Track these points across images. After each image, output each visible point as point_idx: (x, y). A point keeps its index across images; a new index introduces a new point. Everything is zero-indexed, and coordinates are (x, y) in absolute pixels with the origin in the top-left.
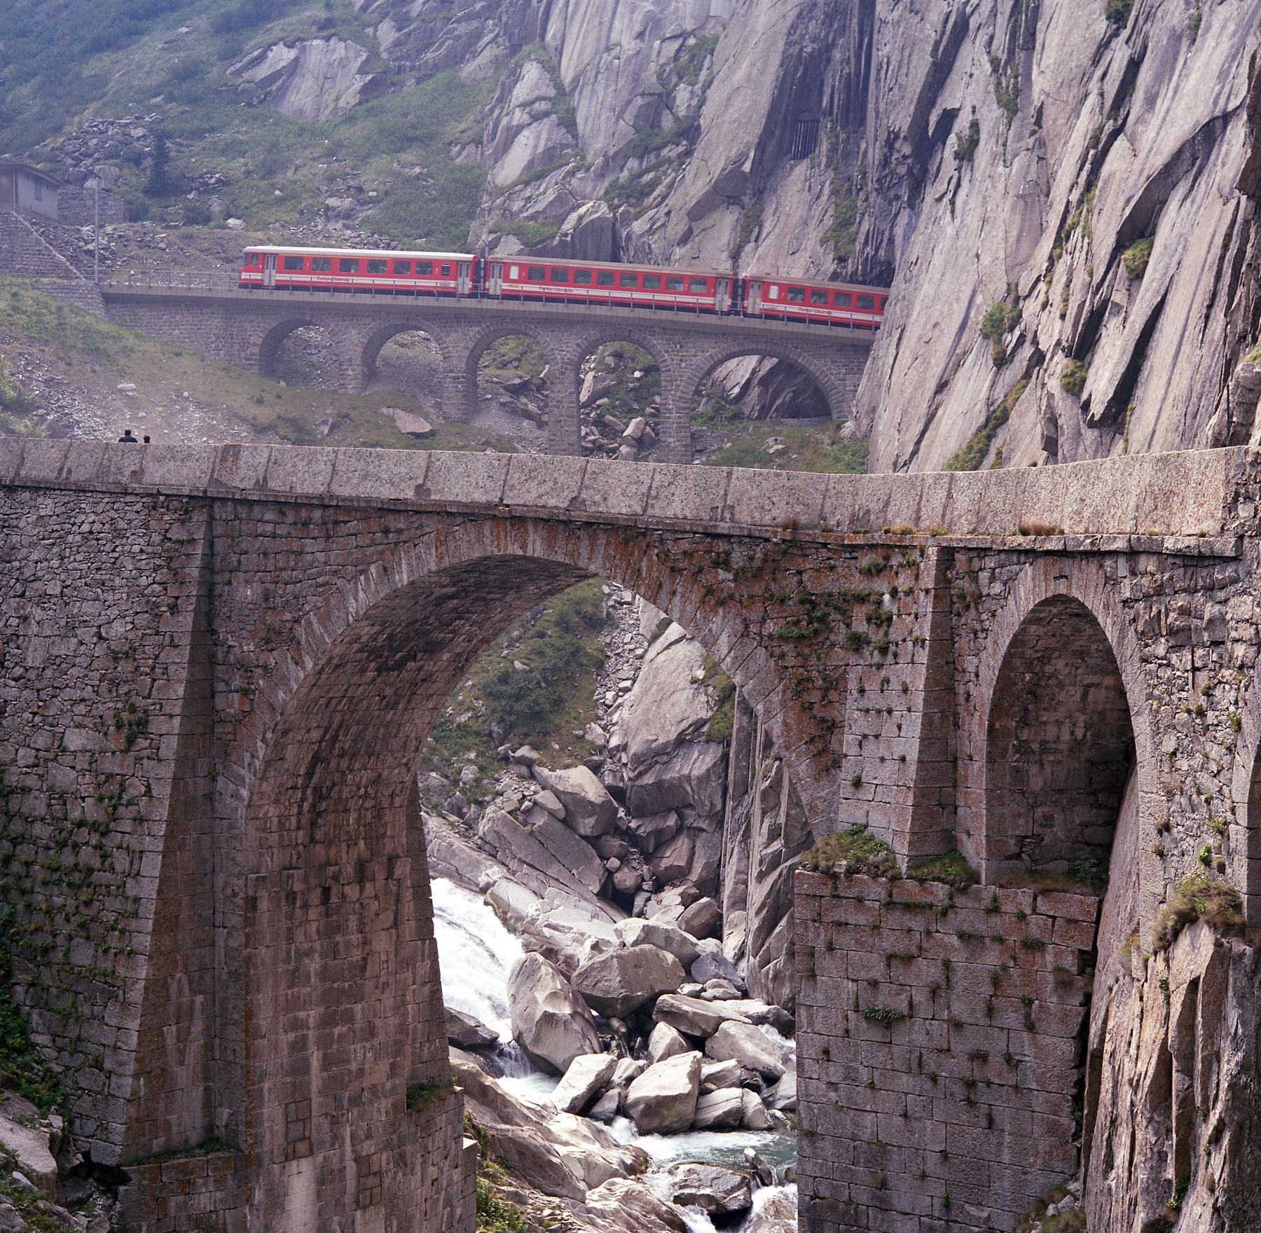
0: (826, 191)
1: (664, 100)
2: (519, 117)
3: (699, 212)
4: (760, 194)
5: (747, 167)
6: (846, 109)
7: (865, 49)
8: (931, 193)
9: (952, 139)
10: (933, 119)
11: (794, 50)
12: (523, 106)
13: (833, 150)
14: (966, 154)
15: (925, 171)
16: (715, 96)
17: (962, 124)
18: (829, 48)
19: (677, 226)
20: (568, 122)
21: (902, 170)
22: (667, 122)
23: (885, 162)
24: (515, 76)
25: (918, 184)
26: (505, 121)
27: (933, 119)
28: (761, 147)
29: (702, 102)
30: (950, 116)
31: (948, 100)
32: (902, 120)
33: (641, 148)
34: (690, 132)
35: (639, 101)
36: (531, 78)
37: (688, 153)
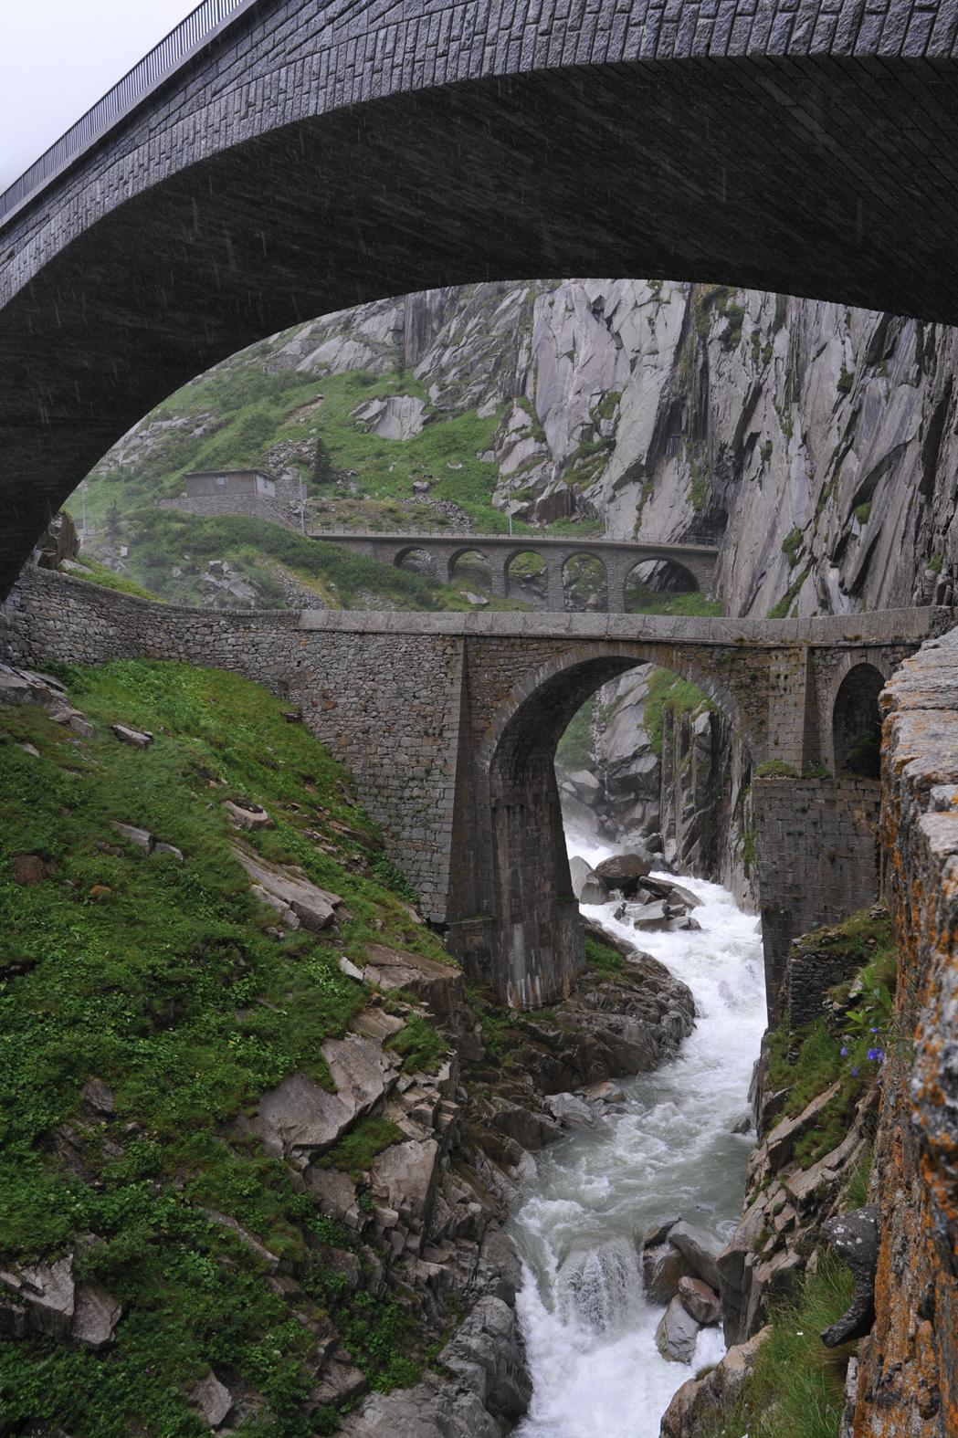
0: (687, 474)
1: (595, 427)
2: (514, 437)
3: (618, 486)
4: (651, 476)
5: (643, 462)
6: (695, 431)
7: (703, 400)
8: (748, 475)
9: (757, 449)
10: (746, 437)
11: (665, 401)
12: (517, 430)
13: (689, 451)
14: (767, 455)
15: (742, 464)
16: (622, 425)
17: (762, 440)
18: (684, 398)
19: (608, 492)
20: (542, 438)
21: (729, 464)
22: (596, 438)
23: (720, 459)
24: (510, 415)
25: (739, 471)
26: (507, 439)
27: (746, 437)
28: (650, 451)
29: (616, 427)
30: (755, 436)
31: (752, 428)
32: (728, 436)
33: (584, 453)
34: (610, 444)
35: (581, 428)
36: (520, 418)
37: (609, 454)
